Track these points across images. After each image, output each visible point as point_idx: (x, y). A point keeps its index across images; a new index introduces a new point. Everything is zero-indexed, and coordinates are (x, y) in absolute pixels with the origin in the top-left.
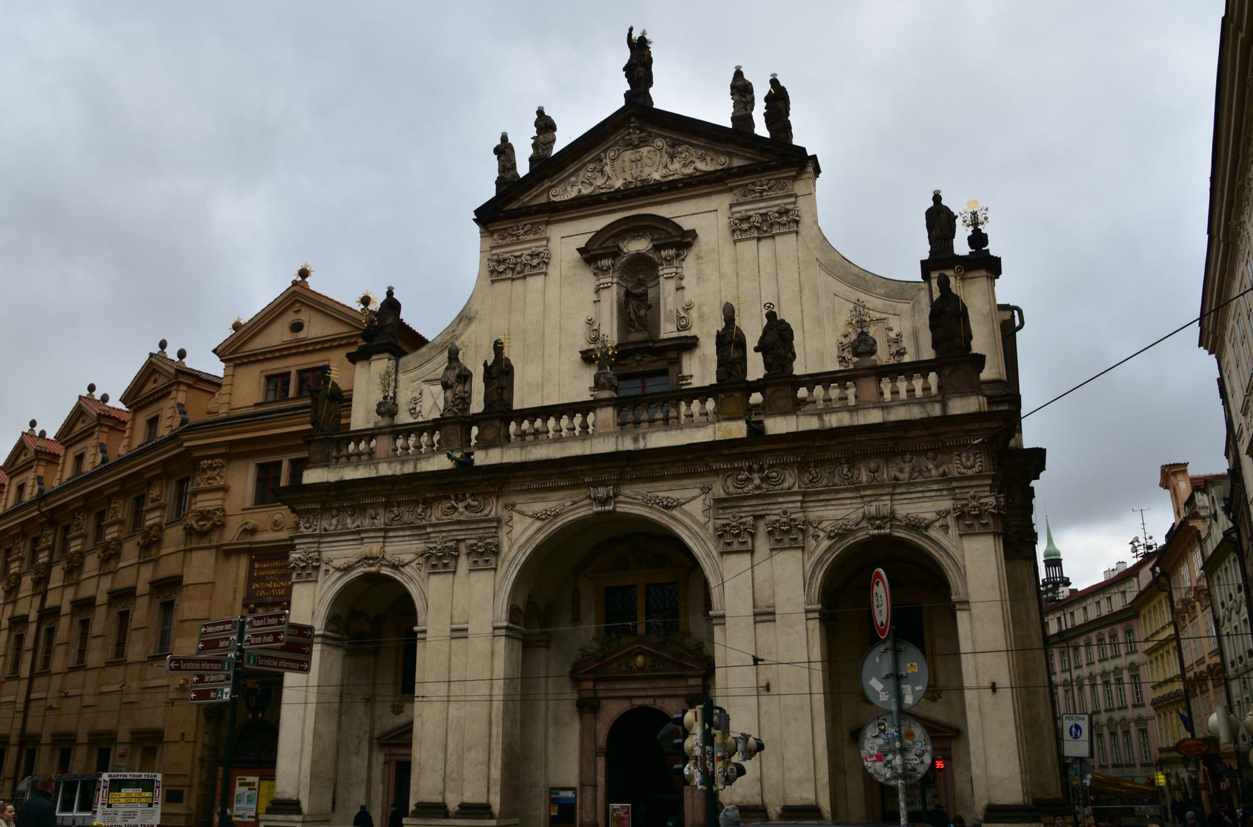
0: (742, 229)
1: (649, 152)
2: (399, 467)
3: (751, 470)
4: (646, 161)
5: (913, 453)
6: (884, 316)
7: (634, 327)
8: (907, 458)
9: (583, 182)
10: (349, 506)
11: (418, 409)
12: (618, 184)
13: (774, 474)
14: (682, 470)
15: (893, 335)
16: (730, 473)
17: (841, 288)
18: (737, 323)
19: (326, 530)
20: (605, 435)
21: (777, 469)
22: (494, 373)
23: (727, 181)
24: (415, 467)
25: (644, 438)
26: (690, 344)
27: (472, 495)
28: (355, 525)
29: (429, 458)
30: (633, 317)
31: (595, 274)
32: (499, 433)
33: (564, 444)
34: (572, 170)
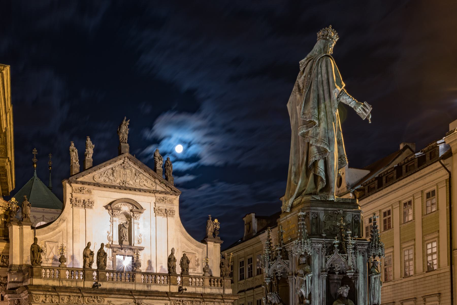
0: (157, 211)
1: (129, 172)
2: (70, 283)
3: (180, 301)
4: (128, 175)
5: (216, 302)
6: (195, 252)
7: (124, 239)
8: (215, 303)
9: (105, 176)
10: (54, 295)
11: (45, 252)
12: (118, 181)
13: (185, 303)
14: (162, 298)
15: (197, 259)
16: (174, 301)
17: (185, 240)
18: (175, 255)
19: (44, 302)
20: (140, 284)
21: (186, 301)
22: (102, 254)
23: (155, 194)
24: (77, 284)
25: (150, 286)
26: (141, 249)
27: (100, 297)
28: (56, 302)
29: (81, 281)
30: (124, 235)
31: (110, 215)
32: (105, 277)
33: (127, 284)
34: (102, 170)
